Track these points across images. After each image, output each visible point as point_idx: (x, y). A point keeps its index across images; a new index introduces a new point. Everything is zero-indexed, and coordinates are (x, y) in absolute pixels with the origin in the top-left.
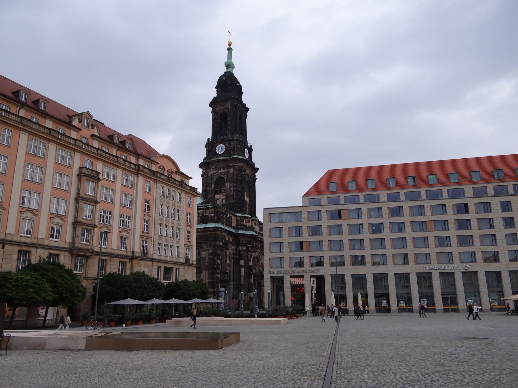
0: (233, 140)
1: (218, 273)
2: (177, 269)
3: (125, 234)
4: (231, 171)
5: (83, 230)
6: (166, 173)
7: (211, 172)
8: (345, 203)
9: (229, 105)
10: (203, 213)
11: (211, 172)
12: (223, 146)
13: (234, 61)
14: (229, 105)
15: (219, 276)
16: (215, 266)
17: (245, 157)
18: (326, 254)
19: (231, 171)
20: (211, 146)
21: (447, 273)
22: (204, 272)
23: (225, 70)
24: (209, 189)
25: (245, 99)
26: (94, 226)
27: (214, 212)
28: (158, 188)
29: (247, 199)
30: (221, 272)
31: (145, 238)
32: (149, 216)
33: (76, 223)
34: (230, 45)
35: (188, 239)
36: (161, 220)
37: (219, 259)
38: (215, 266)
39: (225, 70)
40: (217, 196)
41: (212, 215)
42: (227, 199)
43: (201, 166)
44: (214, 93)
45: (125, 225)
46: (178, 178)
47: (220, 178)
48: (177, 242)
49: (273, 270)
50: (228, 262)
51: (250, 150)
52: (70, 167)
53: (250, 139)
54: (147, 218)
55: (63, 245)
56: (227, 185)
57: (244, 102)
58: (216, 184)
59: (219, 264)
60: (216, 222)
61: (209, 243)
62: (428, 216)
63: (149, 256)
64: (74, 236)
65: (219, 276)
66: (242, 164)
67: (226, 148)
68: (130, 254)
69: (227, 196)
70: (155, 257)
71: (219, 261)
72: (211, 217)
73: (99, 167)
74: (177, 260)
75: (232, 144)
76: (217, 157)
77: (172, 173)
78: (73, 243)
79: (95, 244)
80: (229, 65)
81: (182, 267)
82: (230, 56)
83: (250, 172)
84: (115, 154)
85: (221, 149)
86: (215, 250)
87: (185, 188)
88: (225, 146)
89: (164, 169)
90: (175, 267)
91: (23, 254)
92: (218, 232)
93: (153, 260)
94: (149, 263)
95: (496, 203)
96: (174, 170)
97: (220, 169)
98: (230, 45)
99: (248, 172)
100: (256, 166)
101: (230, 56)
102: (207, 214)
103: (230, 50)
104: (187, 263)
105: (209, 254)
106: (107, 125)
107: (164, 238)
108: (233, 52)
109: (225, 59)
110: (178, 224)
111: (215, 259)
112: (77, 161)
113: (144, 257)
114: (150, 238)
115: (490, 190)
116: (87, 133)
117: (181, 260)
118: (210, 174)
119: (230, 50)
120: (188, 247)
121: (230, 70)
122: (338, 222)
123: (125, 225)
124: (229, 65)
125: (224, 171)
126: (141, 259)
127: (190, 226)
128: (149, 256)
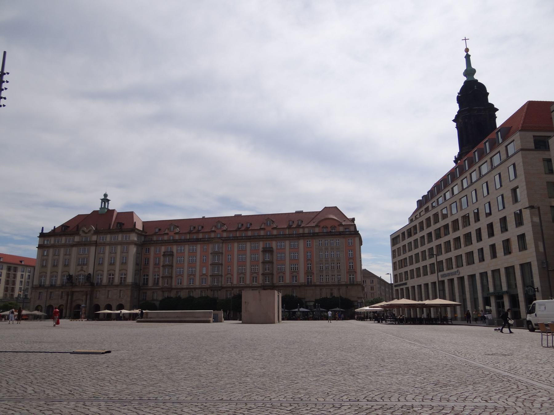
6: (329, 230)
23: (465, 79)
28: (316, 243)
34: (467, 50)
39: (465, 79)
55: (258, 285)
70: (318, 283)
77: (335, 227)
80: (470, 72)
84: (287, 233)
89: (327, 227)
93: (316, 286)
94: (314, 288)
98: (467, 50)
103: (468, 57)
106: (305, 211)
107: (324, 271)
109: (464, 68)
114: (314, 273)
119: (468, 57)
124: (470, 72)
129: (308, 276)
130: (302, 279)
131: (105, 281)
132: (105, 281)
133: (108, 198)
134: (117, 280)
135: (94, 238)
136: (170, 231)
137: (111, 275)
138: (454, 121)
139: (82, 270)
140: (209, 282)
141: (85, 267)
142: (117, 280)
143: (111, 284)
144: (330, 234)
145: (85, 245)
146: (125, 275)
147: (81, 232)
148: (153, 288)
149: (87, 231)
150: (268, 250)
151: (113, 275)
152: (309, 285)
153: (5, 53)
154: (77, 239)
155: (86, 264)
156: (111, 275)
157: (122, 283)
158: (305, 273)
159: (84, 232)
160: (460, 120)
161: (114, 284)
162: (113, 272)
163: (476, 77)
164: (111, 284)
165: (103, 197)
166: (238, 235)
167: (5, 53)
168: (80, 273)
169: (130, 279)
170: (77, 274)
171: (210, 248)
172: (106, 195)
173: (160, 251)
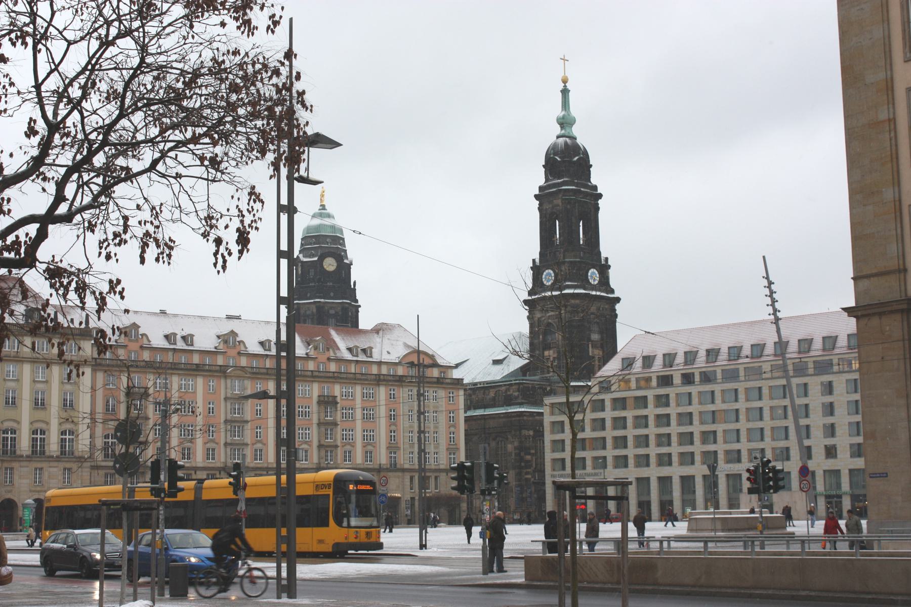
0: (564, 263)
1: (527, 473)
2: (436, 478)
3: (370, 448)
5: (327, 452)
7: (538, 315)
9: (568, 194)
10: (506, 391)
11: (538, 315)
12: (551, 272)
13: (574, 110)
14: (568, 194)
15: (529, 476)
16: (523, 464)
17: (585, 283)
18: (610, 453)
20: (537, 270)
21: (732, 475)
22: (511, 472)
24: (536, 341)
25: (596, 178)
26: (337, 446)
27: (518, 390)
30: (534, 471)
31: (393, 448)
32: (396, 426)
33: (320, 446)
34: (565, 81)
35: (452, 440)
36: (410, 427)
37: (530, 454)
38: (523, 464)
39: (557, 130)
40: (546, 353)
41: (516, 394)
44: (539, 178)
45: (369, 440)
47: (549, 324)
48: (435, 448)
49: (555, 473)
51: (604, 269)
52: (311, 398)
53: (606, 249)
54: (393, 428)
55: (311, 466)
57: (594, 180)
58: (545, 334)
59: (529, 461)
60: (521, 404)
61: (513, 432)
62: (719, 405)
63: (398, 466)
64: (320, 458)
65: (529, 476)
66: (577, 301)
67: (556, 276)
68: (377, 467)
69: (559, 352)
70: (407, 466)
71: (528, 457)
72: (517, 398)
73: (337, 390)
74: (437, 467)
75: (563, 269)
76: (545, 291)
78: (320, 463)
79: (339, 462)
80: (565, 122)
81: (445, 474)
82: (565, 104)
83: (598, 309)
84: (353, 371)
85: (548, 277)
86: (521, 442)
87: (442, 383)
88: (554, 272)
90: (433, 475)
92: (525, 418)
93: (403, 470)
94: (400, 474)
97: (547, 311)
98: (565, 81)
101: (565, 104)
102: (511, 392)
103: (565, 92)
105: (515, 448)
109: (558, 112)
110: (436, 427)
111: (522, 454)
113: (394, 467)
114: (399, 448)
117: (442, 467)
118: (536, 319)
119: (565, 92)
122: (623, 414)
123: (369, 440)
125: (552, 313)
126: (388, 470)
127: (454, 426)
128: (398, 466)
129: (391, 453)
130: (383, 458)
131: (24, 445)
132: (24, 445)
134: (53, 447)
136: (130, 341)
138: (536, 197)
142: (53, 447)
143: (38, 451)
146: (71, 433)
148: (104, 464)
151: (43, 432)
152: (394, 467)
153: (764, 257)
158: (388, 448)
160: (559, 202)
161: (76, 454)
162: (43, 426)
163: (576, 131)
164: (38, 451)
166: (268, 366)
167: (764, 257)
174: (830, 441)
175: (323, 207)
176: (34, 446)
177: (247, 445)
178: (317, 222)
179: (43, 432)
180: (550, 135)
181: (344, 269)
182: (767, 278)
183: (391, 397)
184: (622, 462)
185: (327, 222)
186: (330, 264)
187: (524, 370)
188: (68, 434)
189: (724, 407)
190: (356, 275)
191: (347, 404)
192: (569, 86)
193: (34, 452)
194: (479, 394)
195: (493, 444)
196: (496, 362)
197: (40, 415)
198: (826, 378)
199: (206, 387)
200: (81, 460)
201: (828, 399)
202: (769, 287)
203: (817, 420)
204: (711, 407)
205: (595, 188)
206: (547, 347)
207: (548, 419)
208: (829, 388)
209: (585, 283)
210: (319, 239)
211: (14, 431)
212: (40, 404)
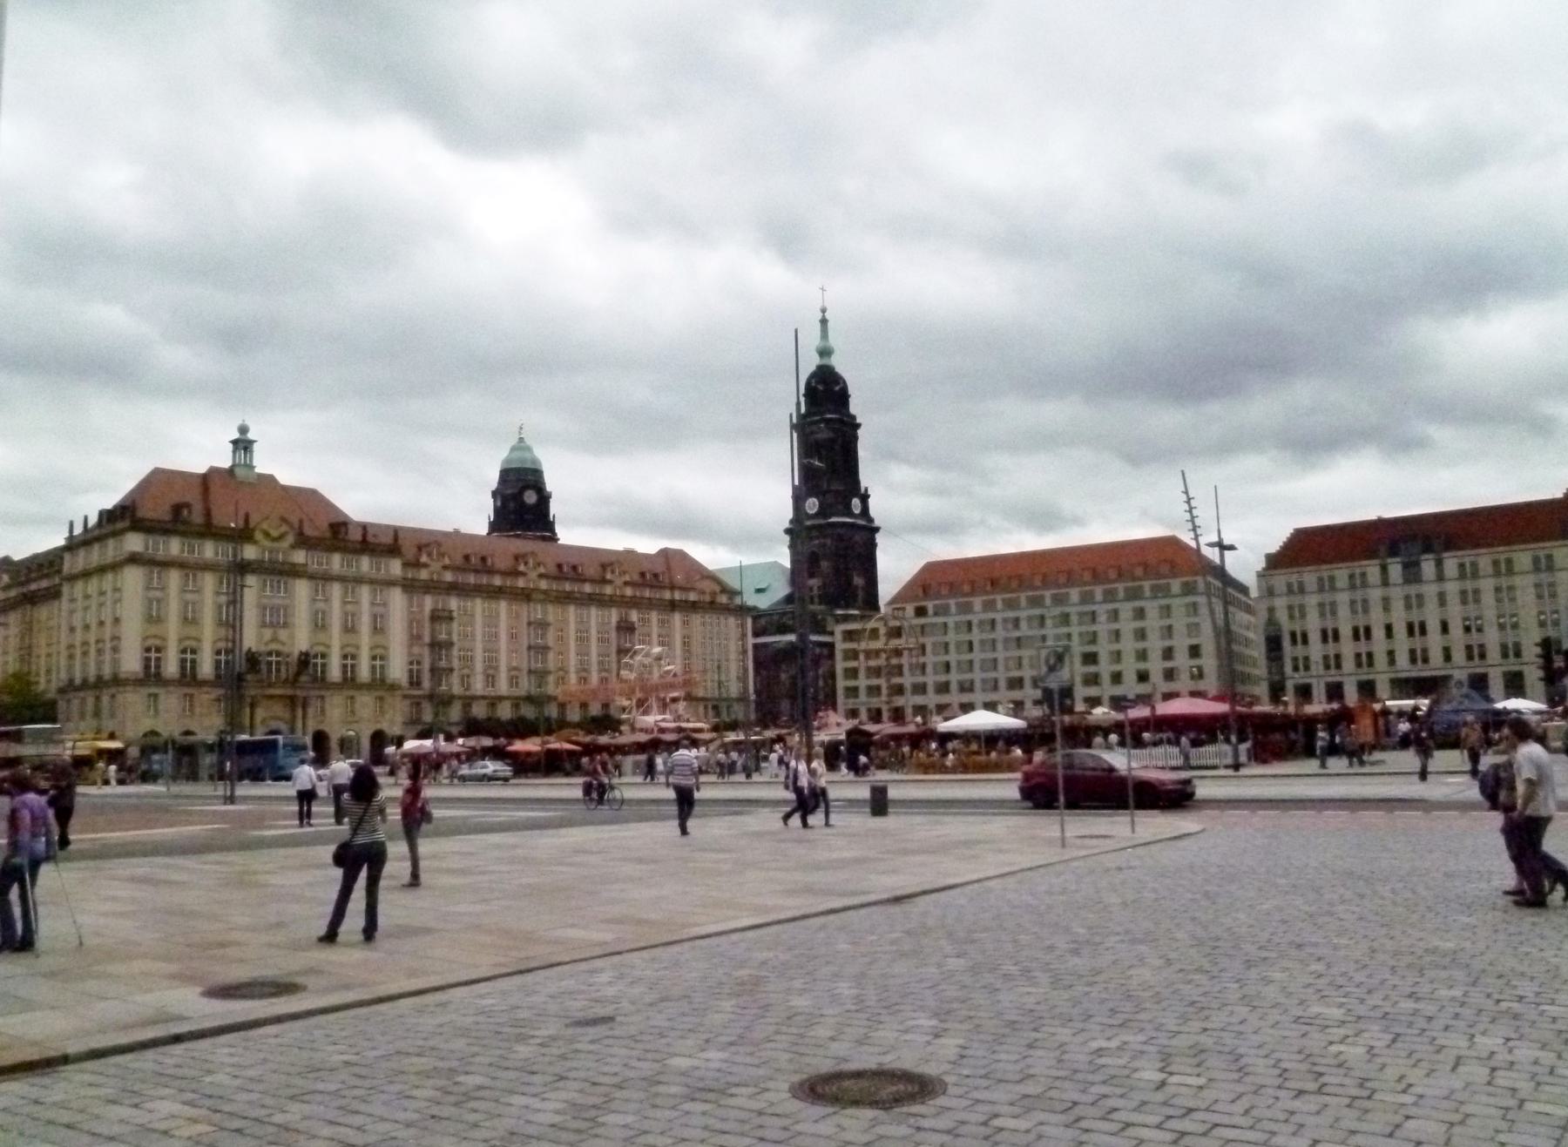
2: (728, 707)
4: (829, 542)
8: (936, 614)
13: (834, 340)
17: (850, 513)
19: (829, 542)
20: (798, 500)
25: (855, 408)
28: (696, 619)
29: (858, 581)
34: (824, 311)
42: (824, 585)
43: (788, 531)
46: (723, 599)
50: (821, 683)
51: (865, 498)
56: (824, 564)
62: (1025, 630)
73: (634, 616)
80: (825, 352)
85: (812, 505)
91: (584, 706)
95: (1102, 610)
96: (717, 588)
98: (824, 311)
99: (857, 538)
100: (877, 523)
103: (824, 322)
104: (743, 699)
108: (830, 325)
112: (614, 615)
115: (1099, 597)
116: (619, 581)
119: (824, 322)
120: (743, 679)
121: (825, 361)
124: (825, 352)
131: (335, 673)
132: (335, 673)
133: (250, 436)
134: (364, 674)
135: (299, 557)
137: (349, 656)
139: (274, 639)
140: (526, 686)
141: (283, 634)
143: (349, 681)
144: (712, 606)
145: (281, 573)
146: (382, 658)
147: (258, 536)
149: (275, 533)
150: (626, 628)
151: (354, 657)
154: (250, 552)
155: (285, 625)
156: (349, 656)
157: (380, 684)
159: (267, 534)
165: (236, 435)
168: (274, 646)
169: (397, 670)
170: (263, 648)
171: (537, 612)
172: (243, 430)
173: (421, 606)
174: (1142, 666)
175: (521, 440)
176: (345, 672)
177: (550, 672)
178: (517, 454)
179: (354, 657)
180: (810, 364)
181: (544, 499)
182: (1186, 492)
183: (685, 623)
184: (920, 689)
185: (527, 455)
186: (530, 498)
187: (789, 599)
188: (380, 657)
189: (1030, 633)
190: (555, 509)
191: (645, 630)
192: (827, 315)
193: (345, 679)
194: (766, 622)
195: (764, 673)
196: (759, 591)
197: (350, 638)
198: (1138, 604)
199: (510, 611)
200: (393, 687)
201: (1139, 624)
202: (1188, 501)
203: (1128, 645)
204: (1017, 634)
205: (854, 417)
206: (812, 575)
207: (840, 646)
208: (1140, 614)
209: (850, 513)
210: (518, 471)
211: (323, 656)
212: (349, 629)
